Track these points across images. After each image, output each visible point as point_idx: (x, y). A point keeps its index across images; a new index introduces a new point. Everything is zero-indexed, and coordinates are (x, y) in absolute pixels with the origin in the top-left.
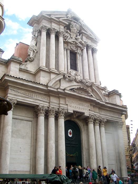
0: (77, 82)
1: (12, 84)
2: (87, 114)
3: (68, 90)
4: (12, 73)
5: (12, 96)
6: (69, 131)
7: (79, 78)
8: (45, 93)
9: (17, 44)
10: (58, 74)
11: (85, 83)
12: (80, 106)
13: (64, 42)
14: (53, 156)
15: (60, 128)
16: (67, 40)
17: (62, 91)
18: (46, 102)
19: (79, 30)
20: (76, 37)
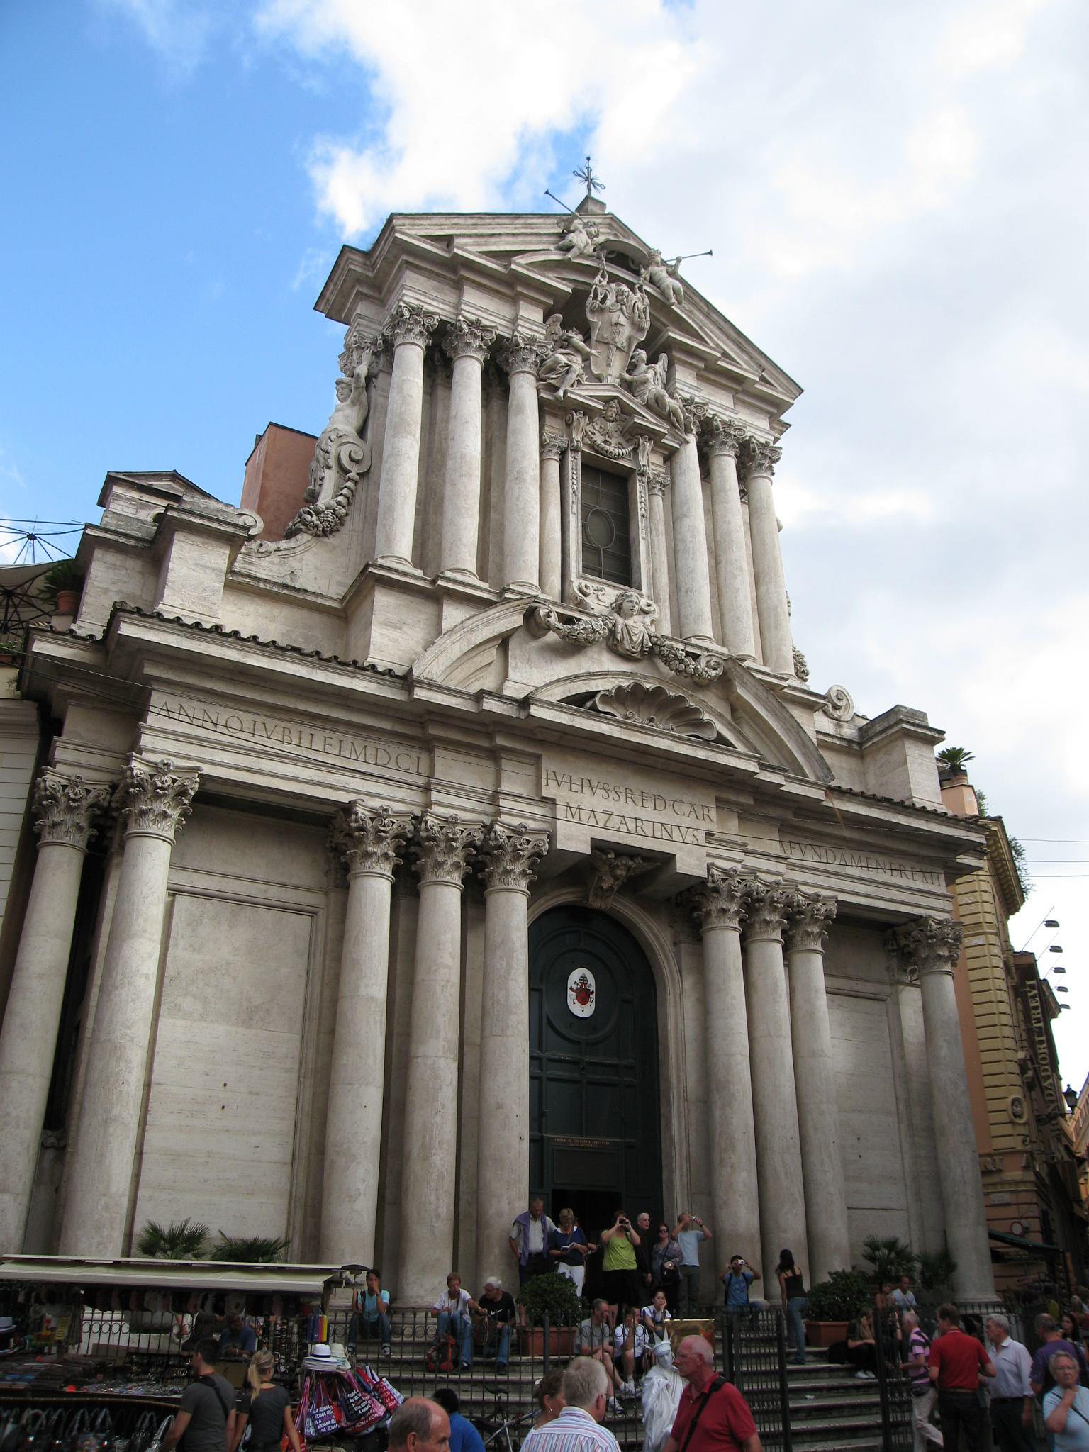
0: (627, 657)
1: (172, 668)
2: (690, 862)
3: (550, 705)
4: (178, 602)
5: (171, 746)
6: (575, 976)
7: (638, 629)
8: (398, 728)
9: (259, 438)
10: (486, 604)
11: (681, 661)
12: (641, 813)
13: (542, 405)
14: (436, 1144)
15: (499, 953)
16: (561, 393)
19: (647, 326)
20: (627, 376)
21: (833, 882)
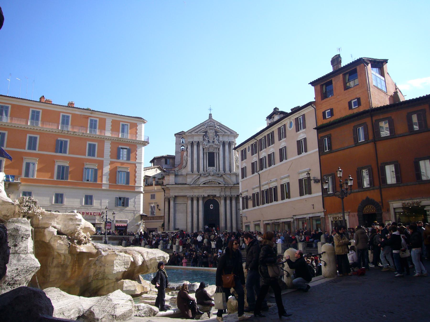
2: (218, 195)
12: (213, 191)
17: (198, 186)
18: (191, 193)
21: (237, 193)
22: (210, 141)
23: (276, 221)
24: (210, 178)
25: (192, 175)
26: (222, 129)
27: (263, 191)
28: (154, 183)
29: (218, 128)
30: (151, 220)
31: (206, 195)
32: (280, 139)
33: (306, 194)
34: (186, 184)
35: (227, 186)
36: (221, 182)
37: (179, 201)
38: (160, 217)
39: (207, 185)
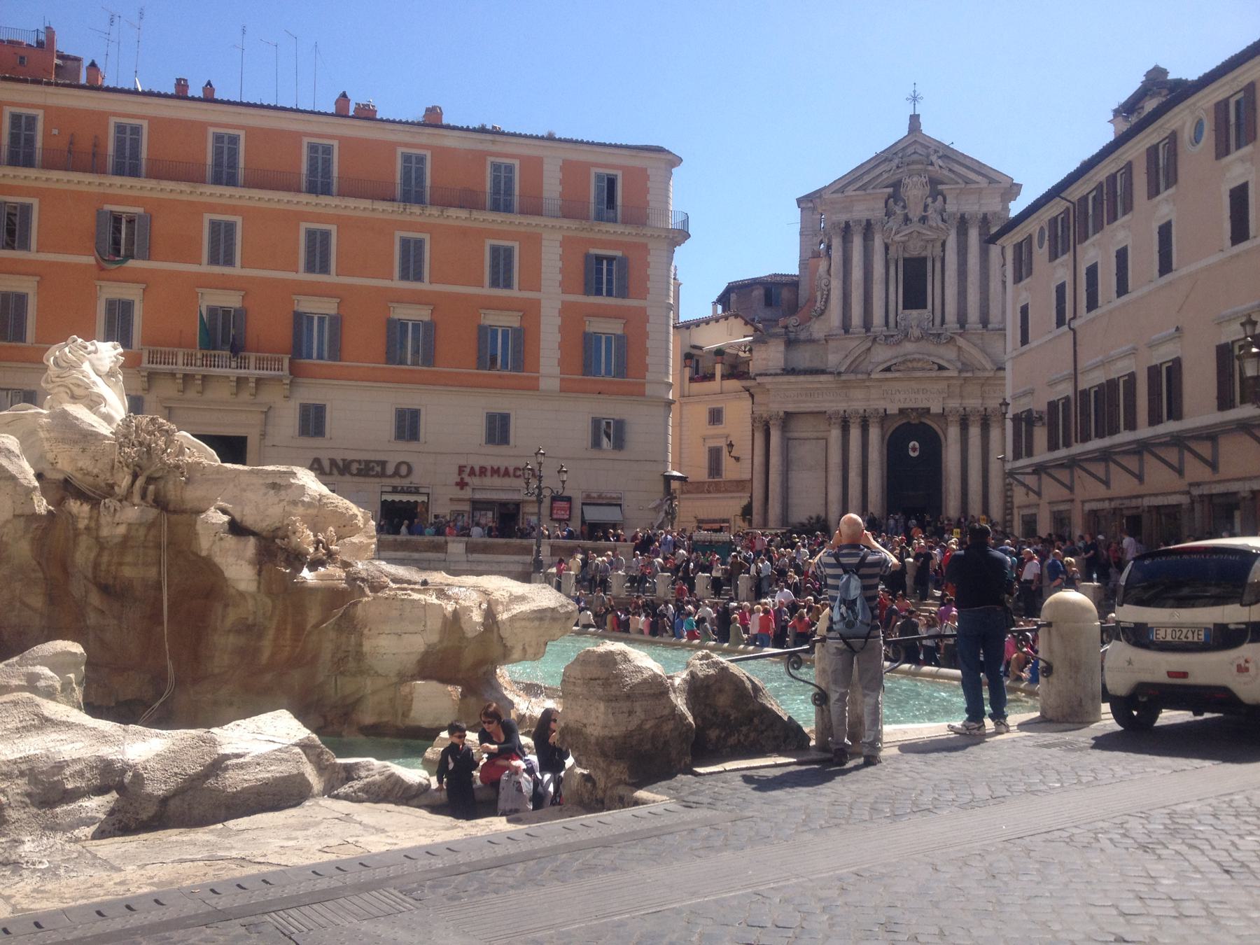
2: (936, 408)
6: (911, 444)
22: (910, 216)
23: (1127, 503)
24: (909, 347)
25: (846, 339)
26: (956, 168)
27: (1085, 393)
28: (719, 369)
29: (940, 167)
30: (709, 492)
31: (893, 409)
32: (1154, 192)
33: (1243, 402)
34: (823, 372)
35: (969, 375)
36: (948, 361)
37: (802, 429)
38: (739, 485)
39: (897, 375)
